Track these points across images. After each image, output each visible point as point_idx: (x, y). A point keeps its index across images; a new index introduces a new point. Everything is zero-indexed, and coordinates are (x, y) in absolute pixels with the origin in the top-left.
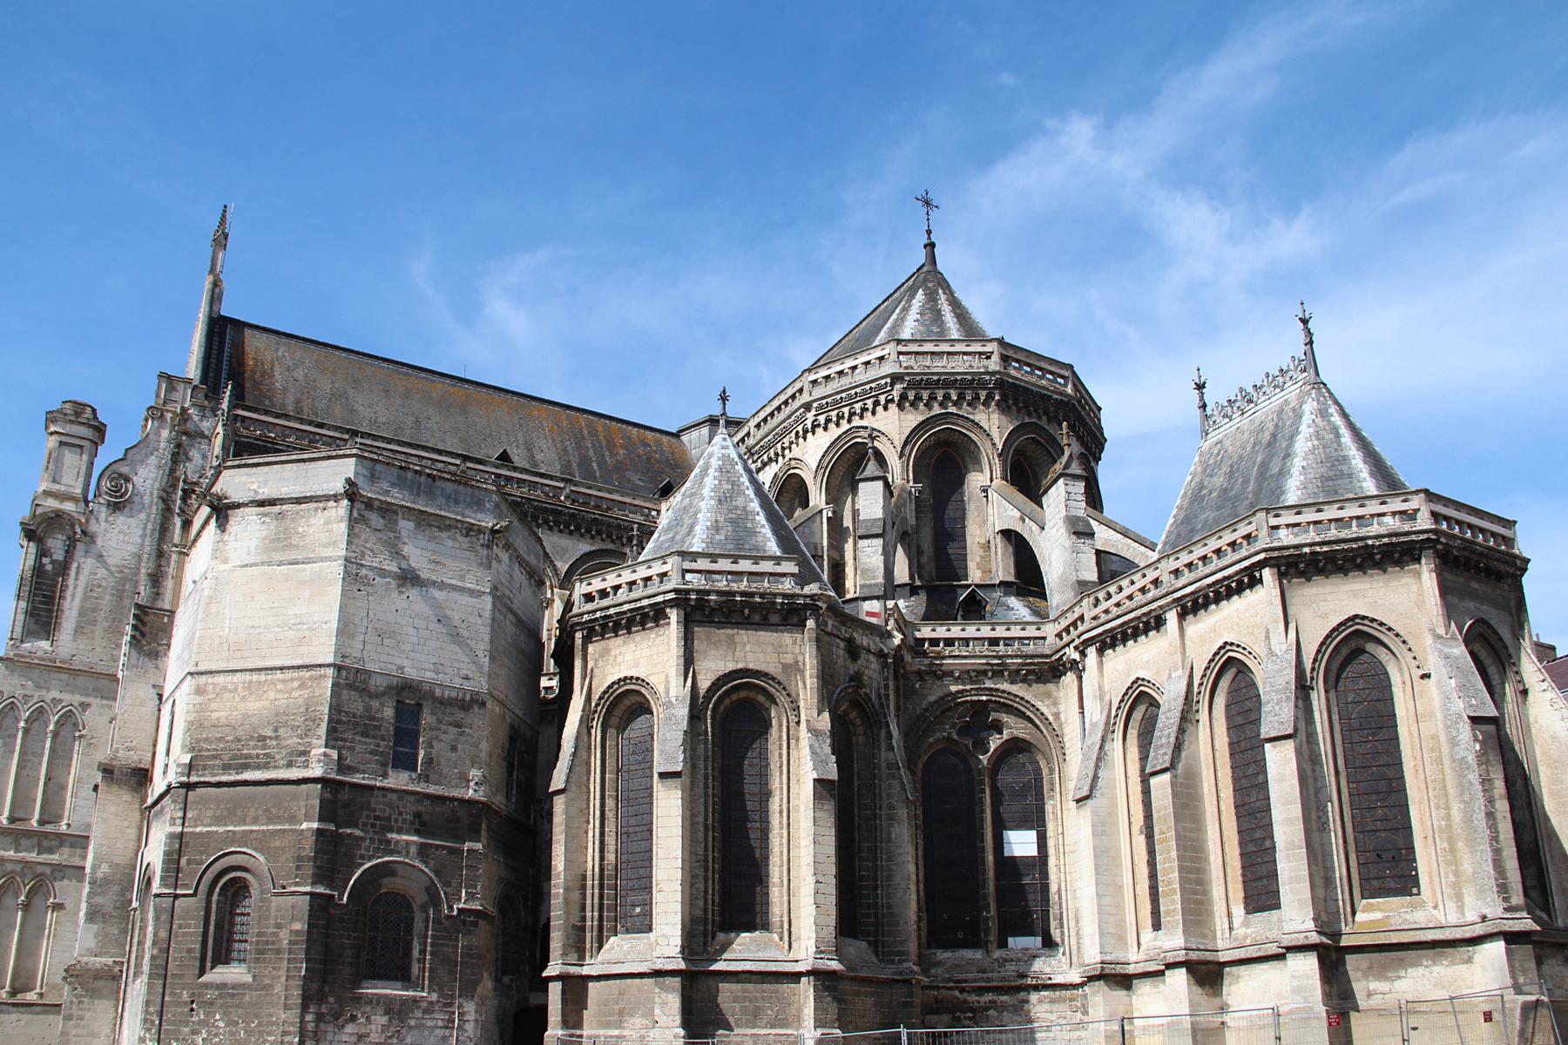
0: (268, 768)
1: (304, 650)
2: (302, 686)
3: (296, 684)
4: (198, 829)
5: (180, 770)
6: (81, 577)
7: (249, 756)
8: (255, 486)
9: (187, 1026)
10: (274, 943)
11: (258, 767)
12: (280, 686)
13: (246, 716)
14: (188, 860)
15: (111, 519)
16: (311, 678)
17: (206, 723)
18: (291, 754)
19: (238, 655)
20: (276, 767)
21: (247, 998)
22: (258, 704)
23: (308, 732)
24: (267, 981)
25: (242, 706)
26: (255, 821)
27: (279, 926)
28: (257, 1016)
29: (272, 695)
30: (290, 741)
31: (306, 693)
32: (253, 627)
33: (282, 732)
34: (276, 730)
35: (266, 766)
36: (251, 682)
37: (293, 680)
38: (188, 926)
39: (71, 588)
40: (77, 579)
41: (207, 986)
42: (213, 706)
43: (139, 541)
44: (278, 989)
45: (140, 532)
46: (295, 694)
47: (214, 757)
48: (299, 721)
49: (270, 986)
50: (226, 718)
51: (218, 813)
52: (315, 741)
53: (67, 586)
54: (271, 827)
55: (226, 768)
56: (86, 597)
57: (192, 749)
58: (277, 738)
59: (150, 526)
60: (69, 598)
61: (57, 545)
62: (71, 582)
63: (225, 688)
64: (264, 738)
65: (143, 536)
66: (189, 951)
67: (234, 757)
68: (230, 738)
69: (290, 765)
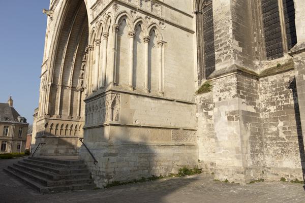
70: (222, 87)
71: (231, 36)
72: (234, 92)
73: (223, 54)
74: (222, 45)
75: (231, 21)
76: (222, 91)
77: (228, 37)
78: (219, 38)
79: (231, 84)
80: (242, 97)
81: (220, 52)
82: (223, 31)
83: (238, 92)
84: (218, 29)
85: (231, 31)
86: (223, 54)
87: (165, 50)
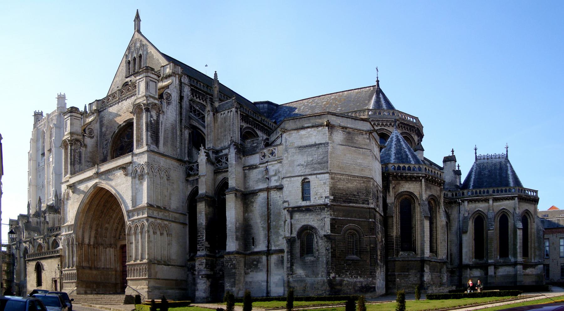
0: (357, 203)
1: (363, 172)
2: (364, 182)
3: (362, 182)
4: (339, 218)
5: (331, 201)
6: (163, 126)
7: (351, 199)
8: (339, 122)
9: (344, 270)
10: (366, 250)
11: (354, 203)
12: (357, 181)
13: (348, 188)
14: (338, 226)
15: (167, 107)
16: (366, 181)
17: (336, 188)
18: (363, 200)
19: (343, 170)
20: (359, 203)
21: (360, 263)
22: (351, 185)
23: (367, 195)
24: (365, 259)
25: (347, 185)
26: (355, 217)
27: (367, 245)
28: (363, 268)
29: (355, 183)
30: (362, 197)
31: (365, 185)
32: (347, 163)
33: (360, 194)
34: (358, 193)
35: (356, 203)
36: (348, 179)
37: (361, 180)
38: (341, 244)
39: (161, 129)
40: (162, 127)
41: (348, 260)
42: (338, 183)
43: (175, 116)
44: (368, 261)
45: (175, 113)
46: (362, 184)
47: (341, 198)
48: (364, 192)
49: (366, 261)
50: (342, 187)
51: (344, 214)
52: (369, 198)
53: (159, 128)
54: (361, 220)
55: (344, 202)
56: (165, 134)
57: (333, 195)
58: (359, 195)
59: (177, 112)
60: (160, 133)
61: (154, 113)
62: (160, 127)
63: (340, 179)
64: (355, 195)
65: (176, 115)
66: (342, 251)
67: (347, 199)
68: (344, 193)
69: (363, 203)
70: (200, 263)
71: (205, 240)
72: (204, 266)
73: (201, 247)
74: (200, 243)
75: (205, 233)
76: (199, 265)
77: (203, 240)
78: (199, 239)
79: (203, 262)
80: (208, 268)
81: (199, 246)
82: (201, 237)
83: (206, 266)
84: (199, 235)
85: (204, 238)
86: (201, 247)
87: (171, 238)
